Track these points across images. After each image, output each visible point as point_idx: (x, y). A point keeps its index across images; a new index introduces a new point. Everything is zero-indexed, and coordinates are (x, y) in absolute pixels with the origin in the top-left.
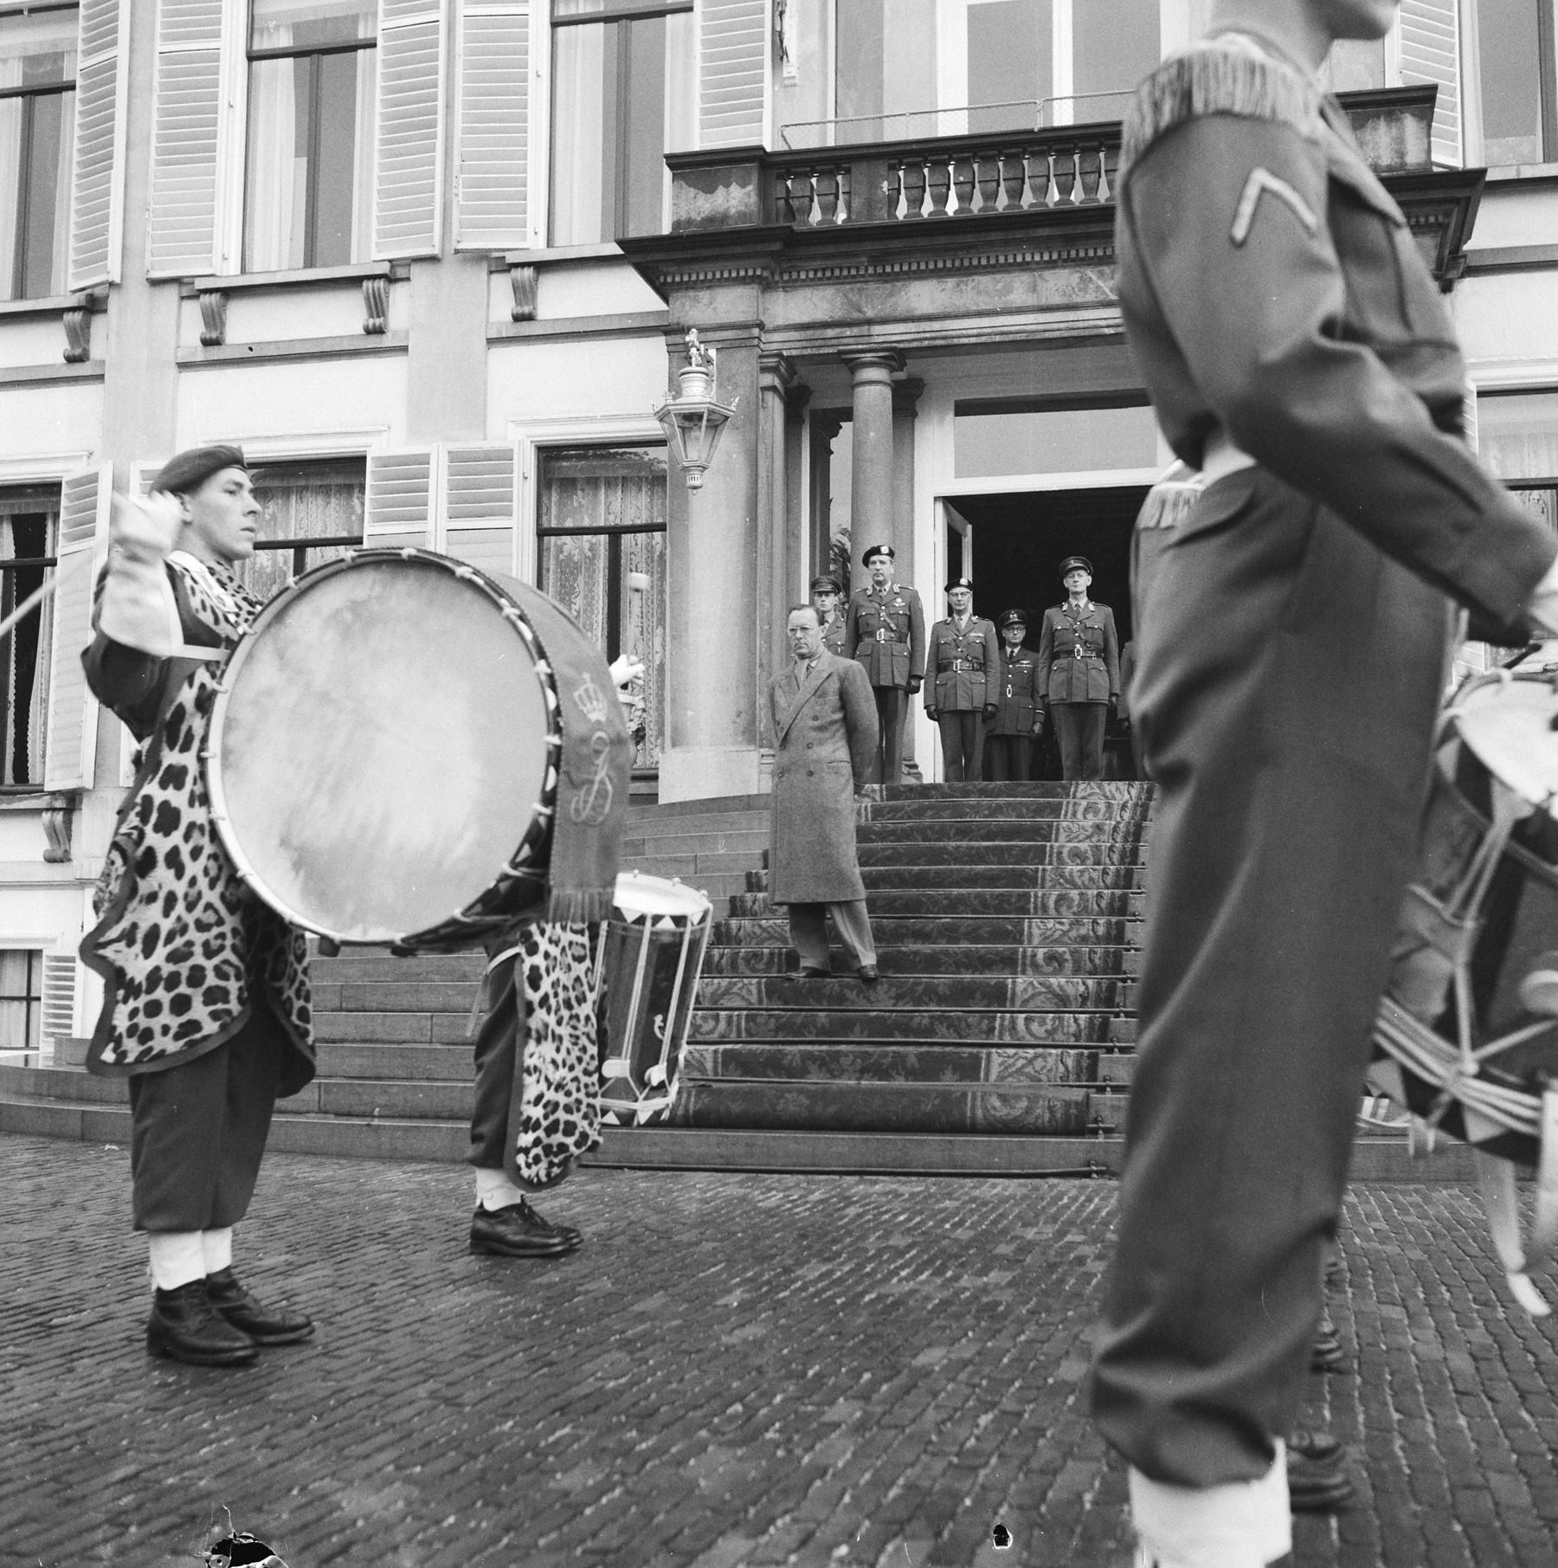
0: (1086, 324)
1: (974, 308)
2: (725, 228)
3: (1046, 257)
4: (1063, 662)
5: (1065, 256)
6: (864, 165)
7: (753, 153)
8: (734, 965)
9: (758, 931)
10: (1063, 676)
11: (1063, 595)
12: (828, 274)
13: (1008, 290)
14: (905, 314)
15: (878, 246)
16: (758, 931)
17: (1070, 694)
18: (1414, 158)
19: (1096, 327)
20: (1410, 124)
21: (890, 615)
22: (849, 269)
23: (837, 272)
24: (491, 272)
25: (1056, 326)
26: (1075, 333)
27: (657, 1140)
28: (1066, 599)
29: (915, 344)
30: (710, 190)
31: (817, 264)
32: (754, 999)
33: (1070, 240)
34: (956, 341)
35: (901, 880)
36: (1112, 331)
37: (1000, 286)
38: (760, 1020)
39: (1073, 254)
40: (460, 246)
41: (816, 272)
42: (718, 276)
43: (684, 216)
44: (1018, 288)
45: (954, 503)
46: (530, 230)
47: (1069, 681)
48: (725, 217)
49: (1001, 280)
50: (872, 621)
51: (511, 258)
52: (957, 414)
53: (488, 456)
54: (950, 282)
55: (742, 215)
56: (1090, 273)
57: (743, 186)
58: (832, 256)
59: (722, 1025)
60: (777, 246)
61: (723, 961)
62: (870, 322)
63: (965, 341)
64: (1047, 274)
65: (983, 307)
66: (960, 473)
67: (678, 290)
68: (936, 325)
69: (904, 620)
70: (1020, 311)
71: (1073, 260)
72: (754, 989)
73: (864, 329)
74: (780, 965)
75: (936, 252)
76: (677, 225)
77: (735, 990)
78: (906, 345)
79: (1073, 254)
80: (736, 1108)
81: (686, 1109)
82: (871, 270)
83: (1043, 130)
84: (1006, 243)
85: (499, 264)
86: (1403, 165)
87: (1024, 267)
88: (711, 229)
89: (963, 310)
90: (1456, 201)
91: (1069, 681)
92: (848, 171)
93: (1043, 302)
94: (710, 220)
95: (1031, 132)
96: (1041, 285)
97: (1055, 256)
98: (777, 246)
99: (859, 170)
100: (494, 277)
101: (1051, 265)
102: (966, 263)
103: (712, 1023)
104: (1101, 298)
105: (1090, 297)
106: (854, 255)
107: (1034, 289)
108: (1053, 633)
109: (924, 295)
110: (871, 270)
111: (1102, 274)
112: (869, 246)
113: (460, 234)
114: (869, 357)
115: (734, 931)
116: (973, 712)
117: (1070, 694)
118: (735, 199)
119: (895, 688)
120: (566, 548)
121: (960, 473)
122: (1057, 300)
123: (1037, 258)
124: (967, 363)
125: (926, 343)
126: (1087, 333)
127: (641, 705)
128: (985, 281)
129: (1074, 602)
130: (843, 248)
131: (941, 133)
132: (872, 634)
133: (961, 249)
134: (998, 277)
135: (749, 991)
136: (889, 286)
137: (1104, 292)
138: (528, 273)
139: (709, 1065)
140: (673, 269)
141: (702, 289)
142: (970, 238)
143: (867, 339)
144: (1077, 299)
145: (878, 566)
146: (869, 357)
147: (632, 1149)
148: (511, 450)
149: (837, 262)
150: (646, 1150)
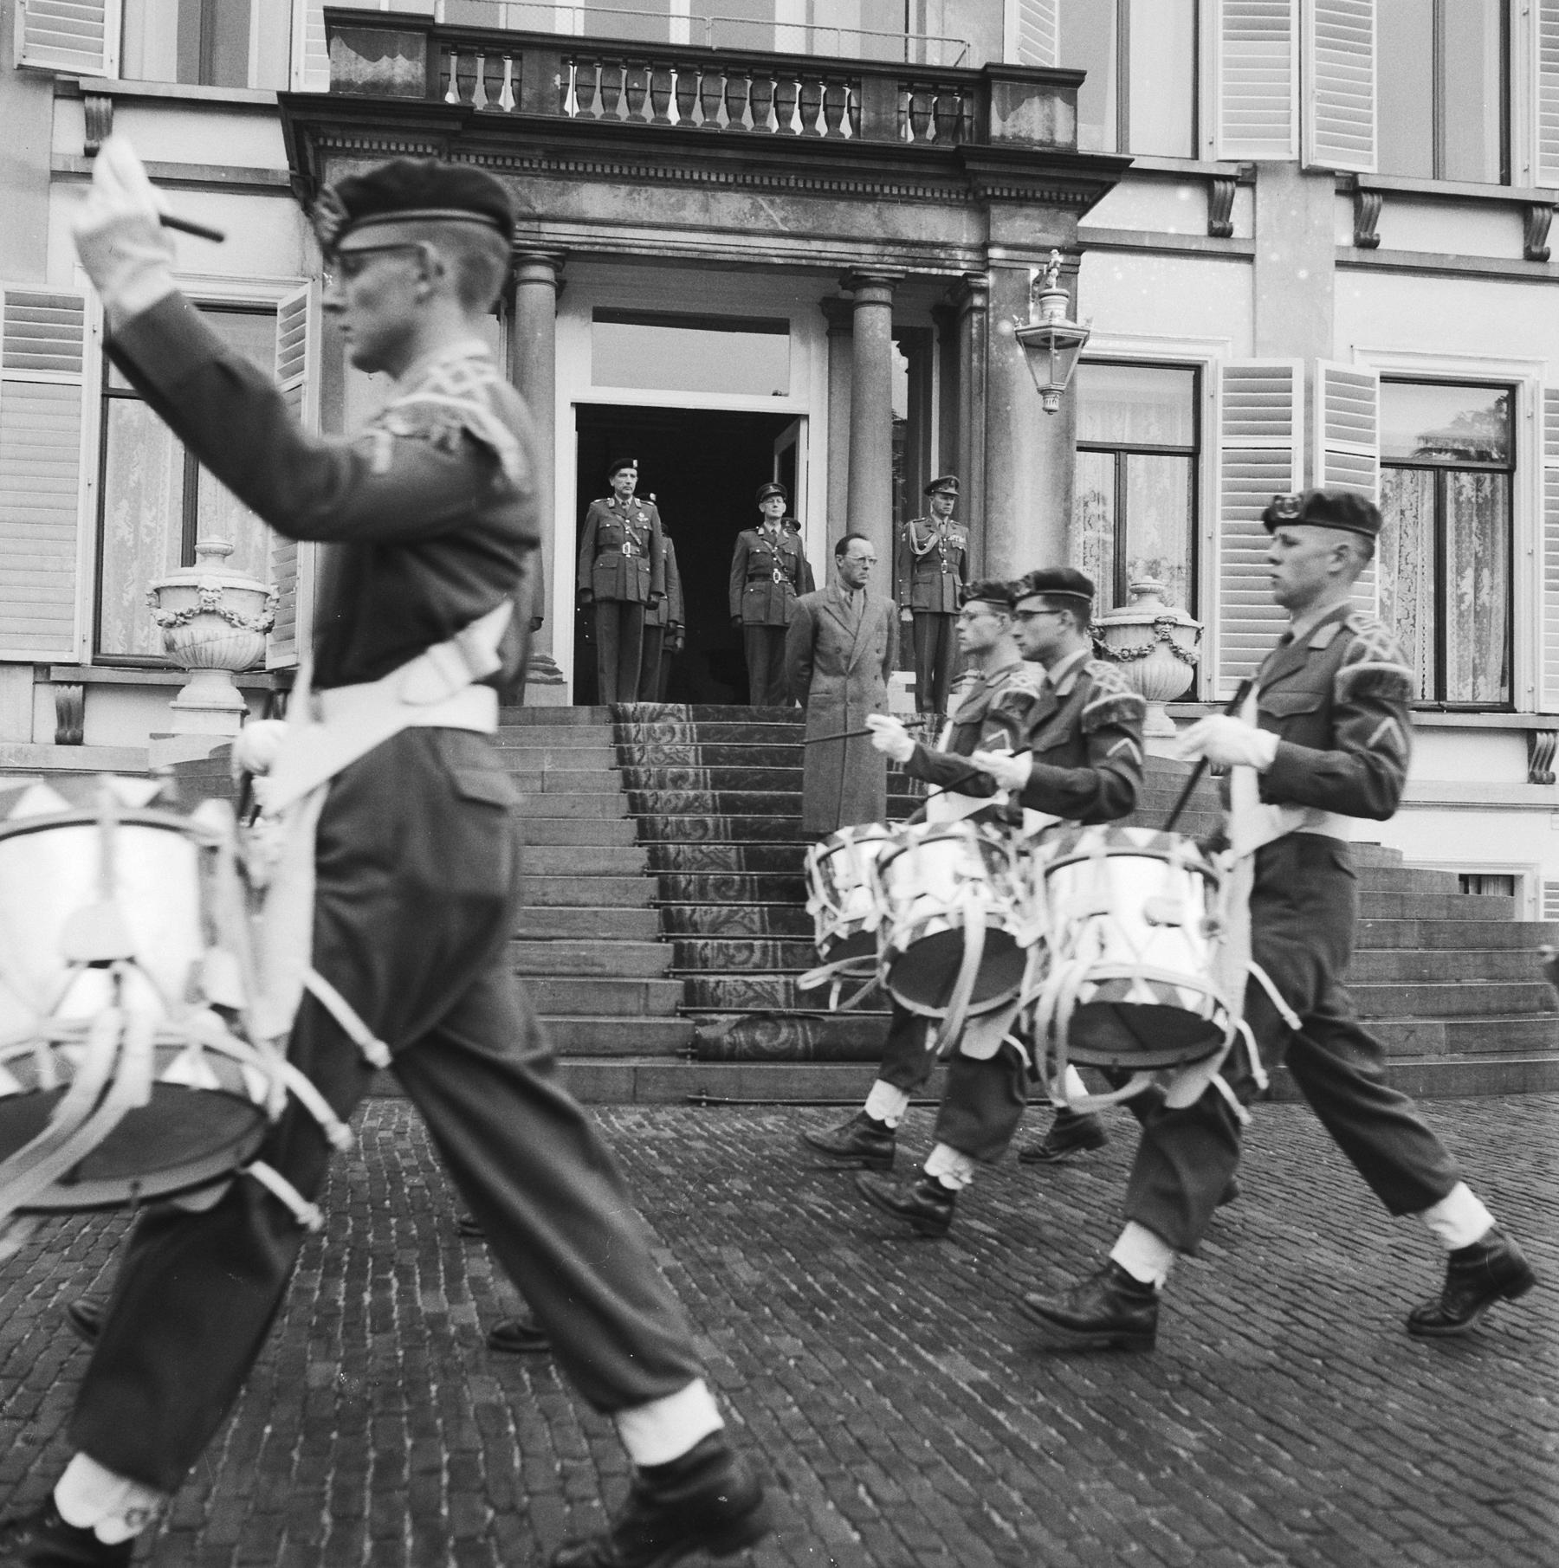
0: (756, 251)
1: (646, 219)
2: (389, 97)
3: (722, 179)
4: (759, 584)
5: (740, 180)
6: (536, 54)
7: (422, 22)
8: (702, 892)
9: (699, 856)
10: (759, 599)
11: (759, 519)
12: (499, 162)
13: (681, 206)
14: (576, 216)
15: (558, 141)
16: (699, 856)
17: (767, 616)
18: (1062, 137)
19: (766, 255)
20: (1059, 103)
21: (635, 529)
22: (522, 161)
23: (509, 162)
24: (56, 97)
25: (727, 249)
26: (745, 258)
27: (807, 1075)
28: (761, 524)
29: (586, 248)
30: (374, 57)
31: (489, 150)
32: (757, 926)
33: (748, 166)
34: (627, 250)
35: (750, 805)
36: (780, 261)
37: (673, 200)
38: (798, 951)
39: (748, 179)
40: (26, 62)
41: (486, 158)
42: (384, 147)
43: (343, 78)
44: (690, 205)
45: (587, 414)
46: (106, 55)
47: (767, 604)
48: (389, 85)
49: (675, 195)
50: (618, 534)
51: (85, 84)
52: (595, 320)
53: (52, 302)
54: (624, 189)
55: (408, 86)
56: (762, 201)
57: (409, 58)
58: (505, 144)
59: (757, 956)
60: (456, 126)
61: (691, 888)
62: (541, 218)
63: (636, 251)
64: (719, 195)
65: (656, 219)
66: (596, 382)
67: (336, 156)
68: (609, 231)
69: (646, 536)
70: (693, 229)
71: (747, 185)
72: (756, 918)
73: (534, 225)
74: (752, 892)
75: (615, 156)
76: (335, 85)
77: (737, 918)
78: (576, 247)
79: (748, 179)
80: (856, 1040)
81: (806, 1042)
82: (545, 165)
83: (720, 50)
84: (685, 158)
85: (71, 90)
86: (1053, 142)
87: (700, 185)
88: (375, 96)
89: (636, 219)
90: (1103, 183)
91: (767, 604)
92: (516, 58)
93: (715, 223)
94: (373, 85)
95: (710, 49)
96: (713, 205)
97: (731, 179)
98: (456, 126)
99: (532, 59)
100: (59, 102)
101: (725, 187)
102: (643, 172)
103: (746, 953)
104: (772, 227)
105: (761, 224)
106: (530, 147)
107: (706, 209)
108: (749, 555)
109: (596, 199)
110: (545, 165)
111: (772, 203)
112: (548, 140)
113: (25, 47)
114: (539, 254)
115: (673, 855)
116: (657, 628)
117: (767, 616)
118: (400, 69)
119: (639, 603)
120: (125, 412)
121: (596, 382)
122: (728, 222)
123: (713, 178)
124: (627, 273)
125: (597, 248)
126: (757, 259)
127: (276, 595)
128: (658, 193)
129: (770, 528)
130: (523, 139)
131: (559, 31)
132: (617, 547)
133: (640, 158)
134: (671, 191)
135: (752, 921)
136: (560, 183)
137: (774, 222)
138: (105, 104)
139: (781, 997)
140: (336, 132)
141: (362, 158)
142: (654, 149)
143: (534, 236)
144: (751, 224)
145: (629, 479)
146: (539, 254)
147: (781, 1085)
148: (81, 300)
149: (507, 151)
150: (795, 1085)
